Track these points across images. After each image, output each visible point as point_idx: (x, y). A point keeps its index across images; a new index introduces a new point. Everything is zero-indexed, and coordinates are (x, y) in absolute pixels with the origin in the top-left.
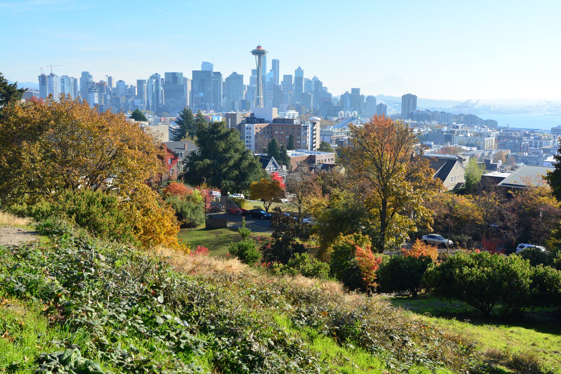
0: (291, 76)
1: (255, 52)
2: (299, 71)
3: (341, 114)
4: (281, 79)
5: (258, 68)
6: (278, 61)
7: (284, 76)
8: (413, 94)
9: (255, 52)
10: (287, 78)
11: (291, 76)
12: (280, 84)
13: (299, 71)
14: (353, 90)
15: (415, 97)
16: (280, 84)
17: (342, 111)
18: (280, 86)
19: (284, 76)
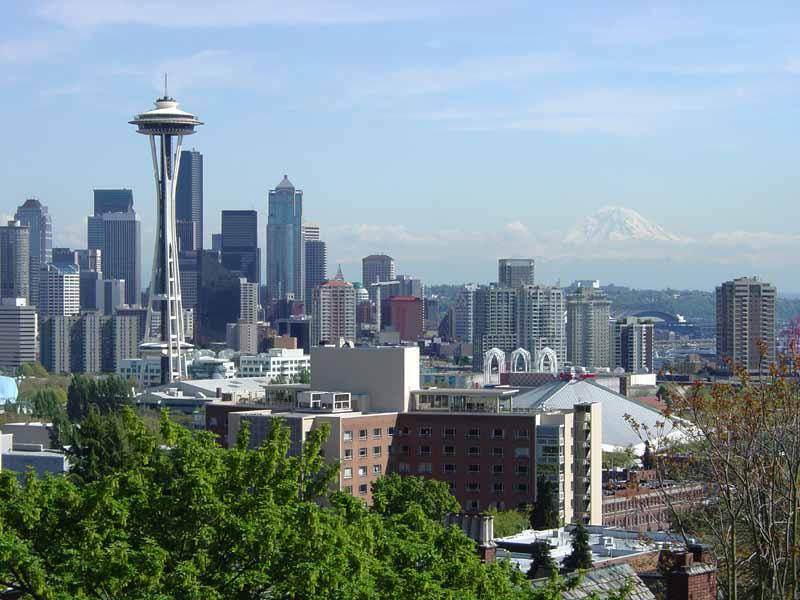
0: (252, 215)
1: (149, 125)
2: (285, 200)
3: (495, 363)
4: (212, 226)
6: (201, 157)
7: (225, 214)
8: (762, 279)
9: (149, 125)
10: (239, 222)
11: (252, 215)
12: (208, 245)
13: (285, 200)
14: (505, 270)
15: (758, 293)
16: (208, 245)
17: (547, 349)
18: (213, 254)
19: (225, 214)
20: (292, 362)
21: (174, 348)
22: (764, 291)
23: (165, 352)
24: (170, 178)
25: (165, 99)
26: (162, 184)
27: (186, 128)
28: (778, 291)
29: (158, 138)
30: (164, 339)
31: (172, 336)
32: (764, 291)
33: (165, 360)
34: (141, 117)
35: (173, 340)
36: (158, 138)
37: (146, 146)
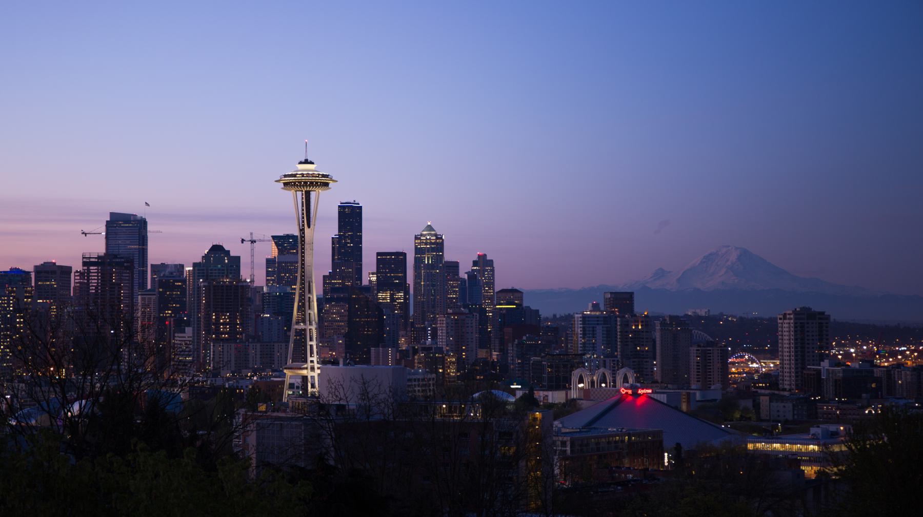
0: (404, 255)
1: (291, 183)
5: (302, 231)
9: (291, 183)
10: (391, 263)
11: (404, 255)
20: (415, 380)
21: (313, 369)
22: (820, 319)
23: (304, 372)
24: (309, 227)
25: (306, 162)
26: (302, 231)
27: (323, 182)
28: (832, 319)
29: (299, 193)
30: (306, 361)
31: (310, 359)
32: (820, 319)
33: (305, 378)
34: (285, 176)
35: (312, 362)
36: (299, 193)
37: (290, 200)
